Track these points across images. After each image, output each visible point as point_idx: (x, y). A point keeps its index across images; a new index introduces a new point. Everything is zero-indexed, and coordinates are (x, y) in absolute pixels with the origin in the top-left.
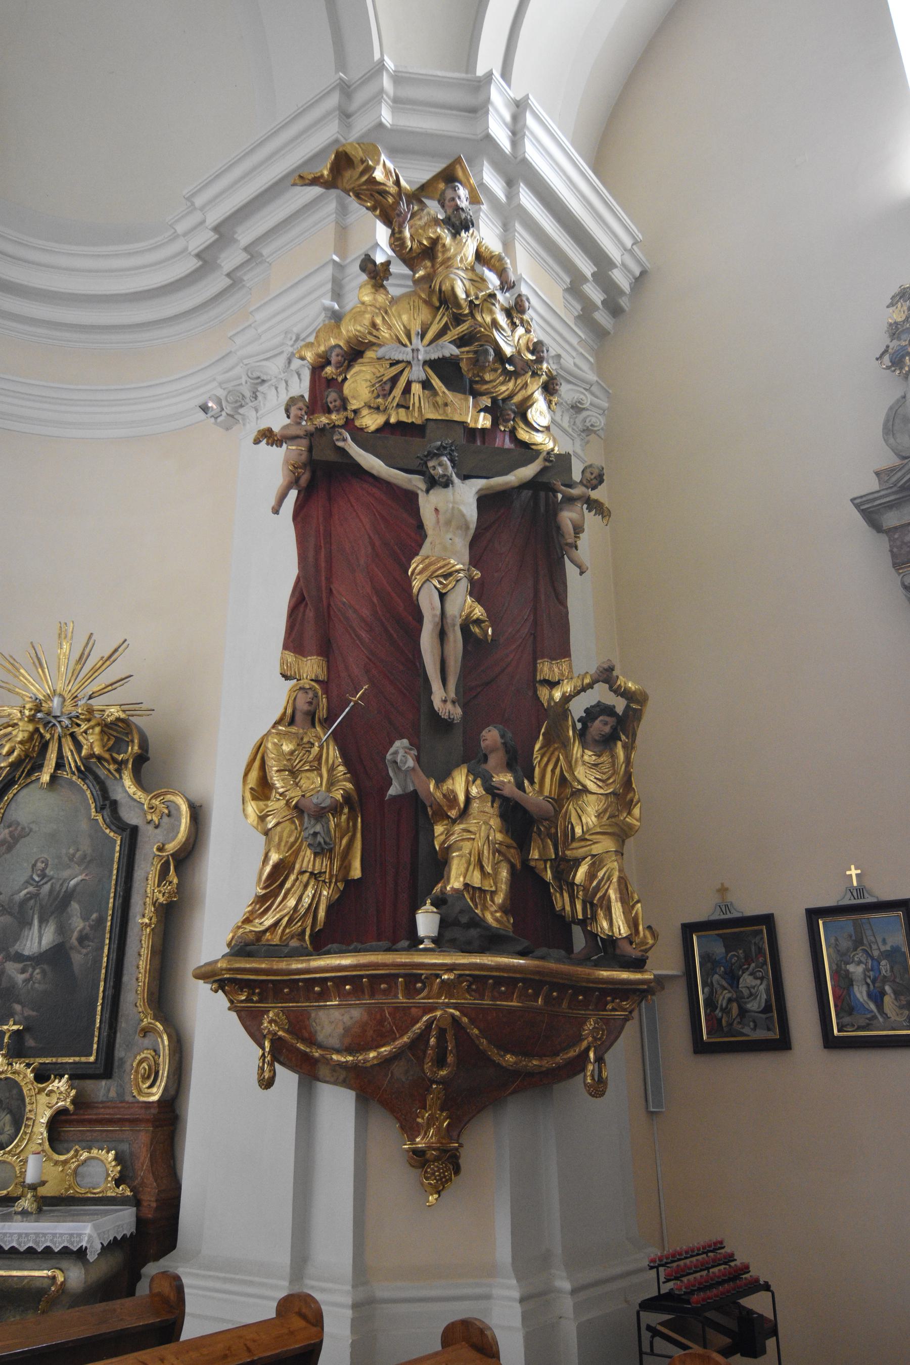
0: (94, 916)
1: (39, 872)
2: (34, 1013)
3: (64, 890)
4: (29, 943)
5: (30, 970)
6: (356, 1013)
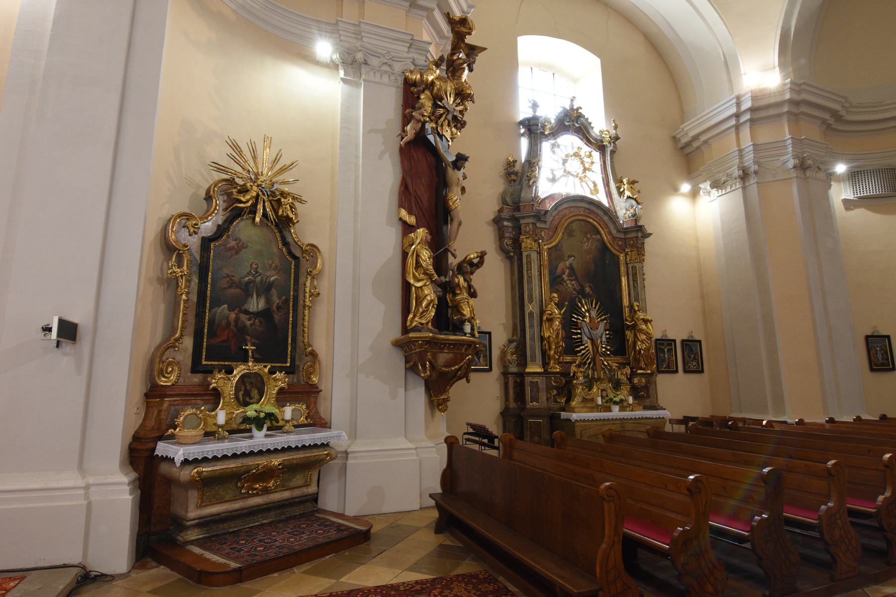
0: (284, 298)
1: (254, 269)
2: (257, 341)
3: (268, 281)
4: (252, 305)
5: (253, 319)
6: (451, 355)
